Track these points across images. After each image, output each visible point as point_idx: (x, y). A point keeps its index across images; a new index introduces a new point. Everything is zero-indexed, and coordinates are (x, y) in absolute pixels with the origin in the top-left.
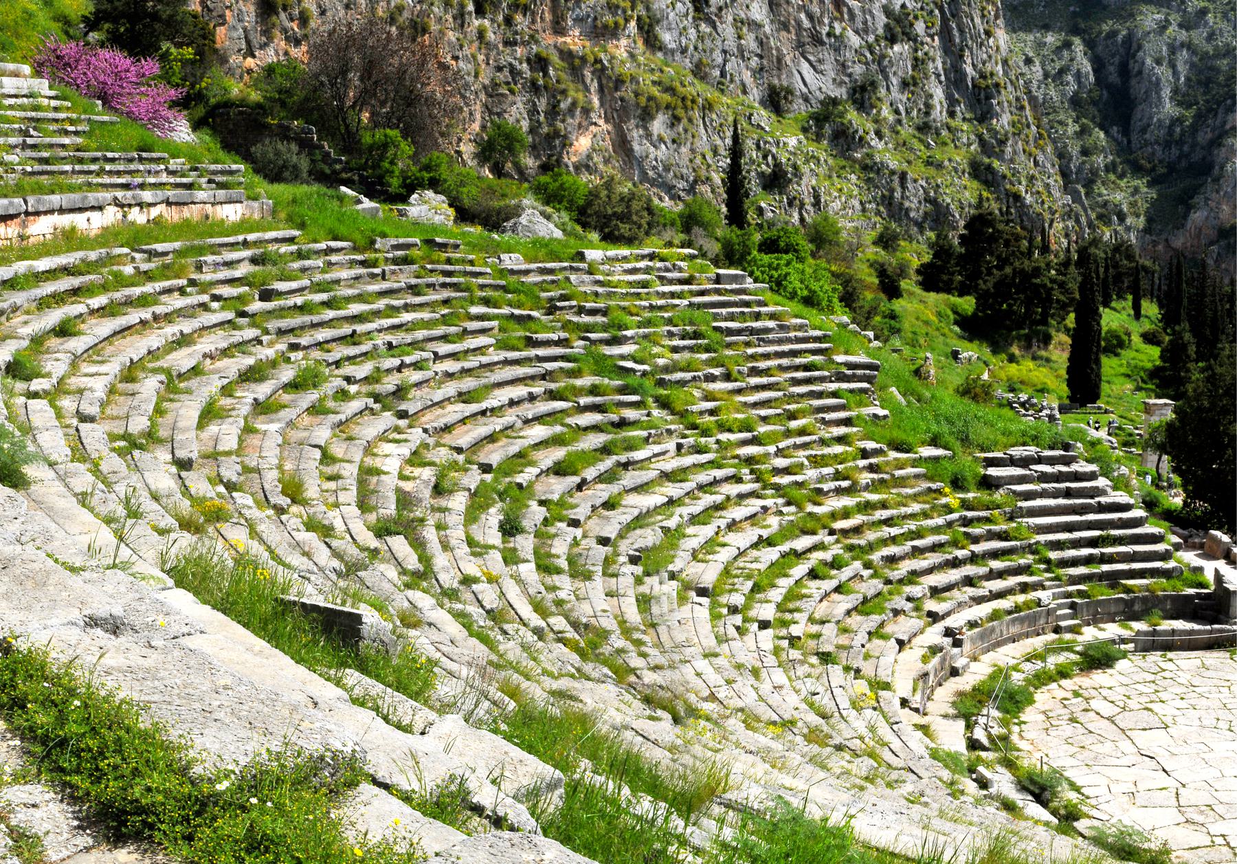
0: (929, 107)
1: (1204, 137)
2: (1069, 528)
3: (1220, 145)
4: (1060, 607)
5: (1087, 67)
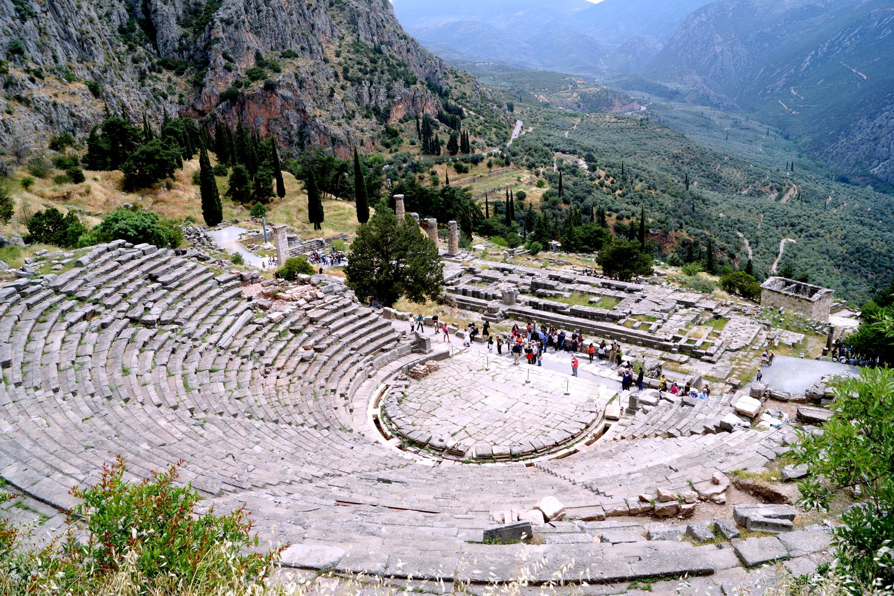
0: (55, 58)
1: (200, 44)
2: (353, 331)
3: (210, 49)
4: (367, 366)
5: (123, 11)
